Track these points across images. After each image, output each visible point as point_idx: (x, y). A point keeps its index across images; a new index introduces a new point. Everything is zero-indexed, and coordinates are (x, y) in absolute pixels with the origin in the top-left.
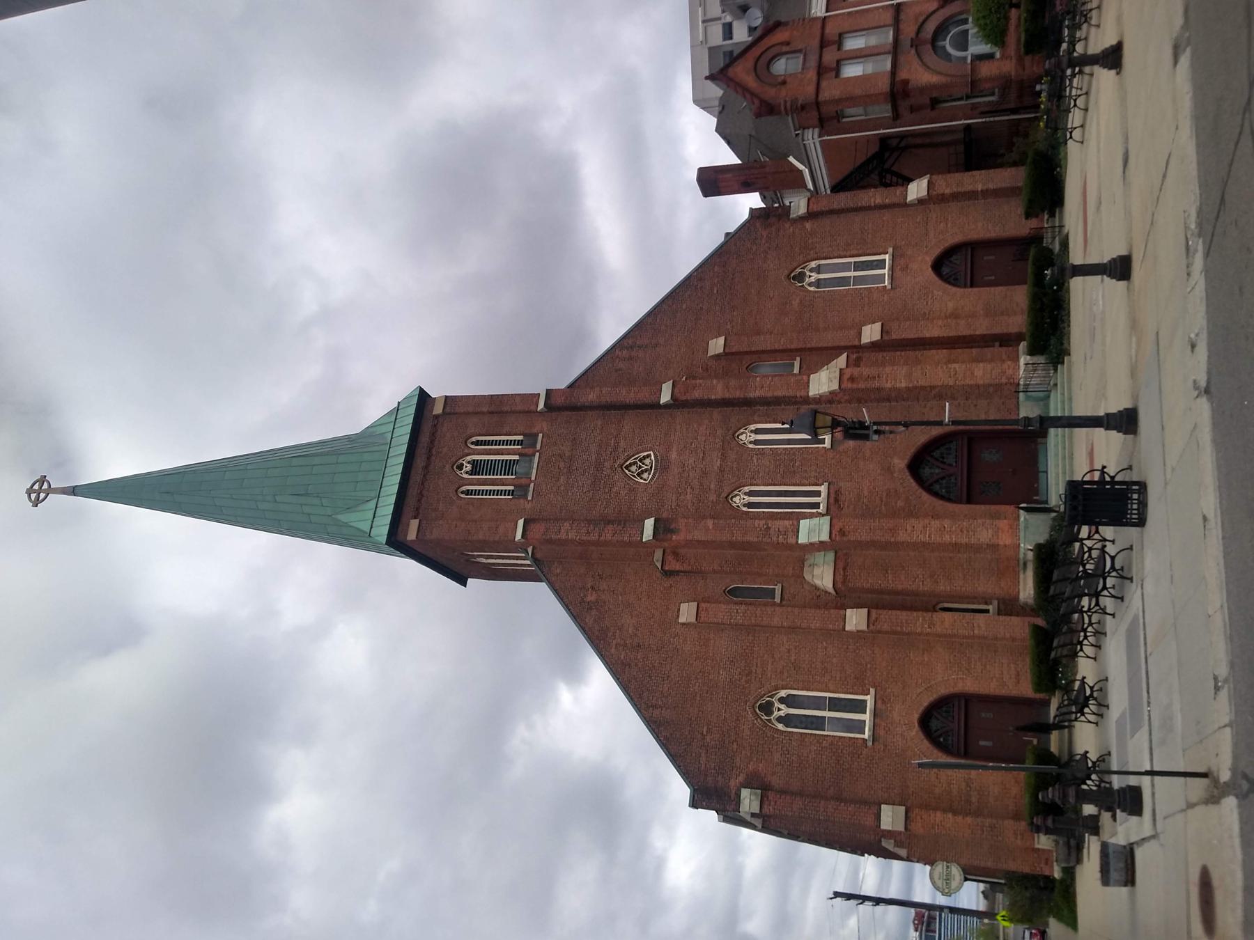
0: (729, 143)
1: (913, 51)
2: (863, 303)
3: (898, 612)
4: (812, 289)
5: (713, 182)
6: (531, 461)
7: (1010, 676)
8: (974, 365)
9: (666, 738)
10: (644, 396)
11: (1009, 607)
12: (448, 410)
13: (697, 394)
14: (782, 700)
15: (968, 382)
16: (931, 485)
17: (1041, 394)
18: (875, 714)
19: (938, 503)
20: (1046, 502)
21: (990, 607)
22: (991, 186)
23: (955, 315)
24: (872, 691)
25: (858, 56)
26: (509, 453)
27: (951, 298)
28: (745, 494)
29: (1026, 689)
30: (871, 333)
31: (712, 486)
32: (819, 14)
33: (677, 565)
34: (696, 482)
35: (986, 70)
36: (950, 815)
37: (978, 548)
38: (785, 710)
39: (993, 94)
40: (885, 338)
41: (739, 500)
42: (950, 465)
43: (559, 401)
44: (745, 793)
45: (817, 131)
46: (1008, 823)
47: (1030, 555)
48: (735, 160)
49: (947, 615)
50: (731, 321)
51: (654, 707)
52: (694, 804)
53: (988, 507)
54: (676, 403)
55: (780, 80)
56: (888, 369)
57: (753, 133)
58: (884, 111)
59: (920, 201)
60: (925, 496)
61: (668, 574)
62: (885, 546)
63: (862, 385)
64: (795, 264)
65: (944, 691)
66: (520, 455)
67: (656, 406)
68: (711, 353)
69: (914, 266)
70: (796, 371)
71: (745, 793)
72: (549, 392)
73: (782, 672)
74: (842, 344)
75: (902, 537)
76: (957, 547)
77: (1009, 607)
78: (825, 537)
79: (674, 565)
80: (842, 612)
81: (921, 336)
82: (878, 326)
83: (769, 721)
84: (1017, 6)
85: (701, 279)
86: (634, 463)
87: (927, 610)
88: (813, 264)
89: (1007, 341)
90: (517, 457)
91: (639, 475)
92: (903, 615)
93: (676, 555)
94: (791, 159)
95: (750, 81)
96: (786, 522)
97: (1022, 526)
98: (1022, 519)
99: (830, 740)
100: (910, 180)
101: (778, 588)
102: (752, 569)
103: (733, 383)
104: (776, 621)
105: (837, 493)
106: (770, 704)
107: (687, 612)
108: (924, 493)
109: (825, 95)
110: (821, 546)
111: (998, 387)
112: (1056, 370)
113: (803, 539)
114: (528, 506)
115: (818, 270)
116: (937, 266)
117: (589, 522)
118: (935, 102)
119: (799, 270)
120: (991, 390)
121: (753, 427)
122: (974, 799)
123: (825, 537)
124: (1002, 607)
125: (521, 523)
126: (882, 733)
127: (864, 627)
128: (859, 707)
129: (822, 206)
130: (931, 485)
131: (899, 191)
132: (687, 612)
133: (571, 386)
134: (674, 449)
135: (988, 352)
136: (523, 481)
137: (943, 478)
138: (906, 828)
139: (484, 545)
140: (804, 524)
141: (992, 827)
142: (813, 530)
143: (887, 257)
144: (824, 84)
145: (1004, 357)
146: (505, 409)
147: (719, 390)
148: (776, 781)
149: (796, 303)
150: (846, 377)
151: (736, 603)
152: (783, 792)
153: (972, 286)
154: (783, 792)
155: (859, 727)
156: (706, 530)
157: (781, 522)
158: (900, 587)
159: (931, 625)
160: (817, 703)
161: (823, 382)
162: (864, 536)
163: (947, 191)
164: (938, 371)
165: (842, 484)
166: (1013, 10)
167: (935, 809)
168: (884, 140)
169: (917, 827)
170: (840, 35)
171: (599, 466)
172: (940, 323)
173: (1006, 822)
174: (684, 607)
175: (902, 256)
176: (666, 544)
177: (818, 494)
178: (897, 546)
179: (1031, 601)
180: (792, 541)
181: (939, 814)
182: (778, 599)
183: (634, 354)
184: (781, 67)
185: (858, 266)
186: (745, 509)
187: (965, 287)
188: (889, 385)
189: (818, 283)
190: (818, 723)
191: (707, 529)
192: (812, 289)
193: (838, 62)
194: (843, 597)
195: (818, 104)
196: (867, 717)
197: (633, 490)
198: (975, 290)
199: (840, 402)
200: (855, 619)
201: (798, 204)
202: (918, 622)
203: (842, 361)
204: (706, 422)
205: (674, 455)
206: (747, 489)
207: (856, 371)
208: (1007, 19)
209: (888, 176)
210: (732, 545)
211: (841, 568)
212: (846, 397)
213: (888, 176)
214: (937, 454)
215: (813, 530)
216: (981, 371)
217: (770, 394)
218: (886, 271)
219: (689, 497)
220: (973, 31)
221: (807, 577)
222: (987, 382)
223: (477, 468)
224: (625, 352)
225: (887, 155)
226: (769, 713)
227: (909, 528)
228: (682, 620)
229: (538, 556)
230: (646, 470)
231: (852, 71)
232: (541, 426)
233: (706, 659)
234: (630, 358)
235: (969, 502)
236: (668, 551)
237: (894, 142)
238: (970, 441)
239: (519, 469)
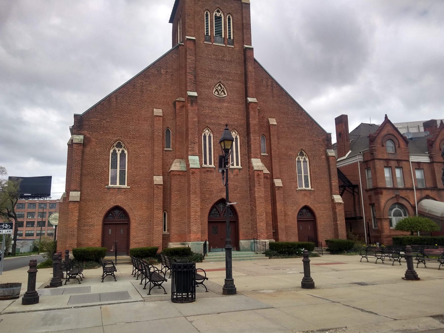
0: (357, 128)
1: (394, 196)
2: (292, 179)
3: (162, 196)
4: (297, 159)
5: (341, 121)
6: (221, 43)
7: (138, 239)
8: (265, 222)
9: (103, 104)
10: (251, 91)
11: (166, 239)
12: (244, 5)
13: (252, 113)
14: (123, 151)
15: (258, 220)
16: (216, 208)
18: (119, 188)
19: (208, 211)
20: (210, 251)
21: (166, 232)
22: (339, 227)
23: (286, 215)
24: (129, 187)
25: (393, 175)
26: (225, 33)
27: (292, 213)
28: (210, 135)
29: (133, 246)
30: (278, 183)
31: (212, 121)
32: (410, 159)
33: (179, 107)
34: (214, 114)
35: (386, 224)
36: (77, 219)
37: (189, 226)
38: (119, 153)
39: (375, 227)
40: (276, 188)
41: (207, 132)
43: (248, 54)
44: (82, 137)
45: (362, 160)
46: (75, 242)
47: (187, 246)
48: (350, 131)
49: (161, 215)
50: (283, 127)
51: (116, 99)
52: (76, 116)
53: (207, 229)
54: (248, 104)
55: (384, 144)
56: (263, 189)
57: (361, 137)
58: (370, 185)
59: (333, 200)
60: (211, 205)
61: (174, 104)
62: (189, 191)
63: (256, 179)
64: (307, 152)
65: (131, 215)
66: (224, 38)
67: (246, 96)
68: (270, 119)
69: (306, 198)
70: (262, 154)
71: (82, 137)
72: (252, 49)
73: (135, 151)
74: (274, 172)
75: (192, 196)
76: (189, 218)
77: (166, 239)
78: (191, 166)
79: (178, 106)
80: (161, 174)
81: (277, 202)
82: (281, 185)
83: (114, 146)
84: (412, 234)
85: (301, 114)
86: (222, 88)
87: (164, 207)
88: (307, 159)
89: (275, 235)
90: (223, 36)
91: (217, 90)
92: (161, 198)
93: (183, 107)
94: (350, 152)
95: (384, 133)
96: (197, 151)
97: (198, 242)
98: (201, 242)
99: (107, 171)
100: (341, 195)
101: (171, 149)
102: (178, 138)
103: (257, 128)
104: (156, 148)
105: (211, 171)
106: (121, 147)
107: (158, 112)
108: (212, 205)
109: (377, 162)
110: (188, 165)
111: (256, 231)
112: (263, 253)
113: (190, 157)
114: (201, 42)
115: (305, 161)
116: (306, 207)
117: (195, 68)
118: (372, 205)
119: (305, 154)
121: (238, 137)
122: (86, 228)
123: (191, 166)
124: (166, 236)
125: (194, 38)
126: (111, 191)
127: (155, 183)
128: (122, 182)
129: (332, 162)
130: (216, 208)
131: (337, 191)
132: (158, 112)
133: (255, 60)
134: (228, 105)
135: (271, 228)
136: (212, 39)
138: (70, 201)
139: (184, 24)
140: (197, 158)
141: (73, 235)
142: (194, 161)
143: (310, 188)
144: (382, 162)
145: (269, 234)
146: (245, 31)
147: (253, 122)
148: (88, 149)
149: (291, 153)
150: (259, 173)
151: (163, 132)
152: (83, 152)
153: (298, 221)
154: (83, 152)
155: (114, 182)
156: (193, 117)
157: (197, 149)
158: (172, 197)
159: (157, 209)
160: (122, 165)
161: (257, 164)
162: (192, 181)
163: (337, 210)
164: (262, 209)
165: (215, 173)
166: (409, 233)
167: (80, 213)
168: (357, 186)
169: (71, 206)
170: (402, 167)
171: (220, 72)
172: (283, 209)
173: (76, 240)
174: (161, 111)
175: (310, 194)
176: (187, 102)
177: (210, 163)
178: (189, 195)
179: (169, 247)
180: (190, 153)
181: (78, 214)
182: (165, 149)
183: (269, 87)
184: (389, 144)
185: (306, 177)
186: (203, 134)
187: (297, 218)
188: (256, 189)
189: (299, 162)
190: (114, 166)
191: (193, 118)
192: (297, 159)
193: (391, 167)
194: (168, 175)
195: (374, 159)
196: (118, 185)
197: (210, 87)
198: (296, 222)
199: (249, 171)
200: (158, 180)
201: (332, 153)
202: (158, 203)
203: (266, 171)
204: (240, 117)
205: (225, 104)
206: (212, 135)
207: (262, 177)
208: (407, 231)
209: (342, 189)
210: (187, 129)
211: (180, 173)
212: (251, 174)
213: (342, 189)
215: (194, 161)
216: (262, 225)
217: (252, 143)
218: (304, 188)
219: (208, 111)
220: (403, 218)
221: (176, 160)
223: (218, 19)
224: (270, 83)
225: (352, 188)
226: (117, 146)
227: (196, 199)
228: (155, 110)
229: (180, 47)
230: (219, 93)
231: (387, 173)
232: (237, 47)
233: (139, 120)
234: (267, 86)
235: (209, 222)
236: (184, 103)
237: (356, 190)
239: (218, 38)
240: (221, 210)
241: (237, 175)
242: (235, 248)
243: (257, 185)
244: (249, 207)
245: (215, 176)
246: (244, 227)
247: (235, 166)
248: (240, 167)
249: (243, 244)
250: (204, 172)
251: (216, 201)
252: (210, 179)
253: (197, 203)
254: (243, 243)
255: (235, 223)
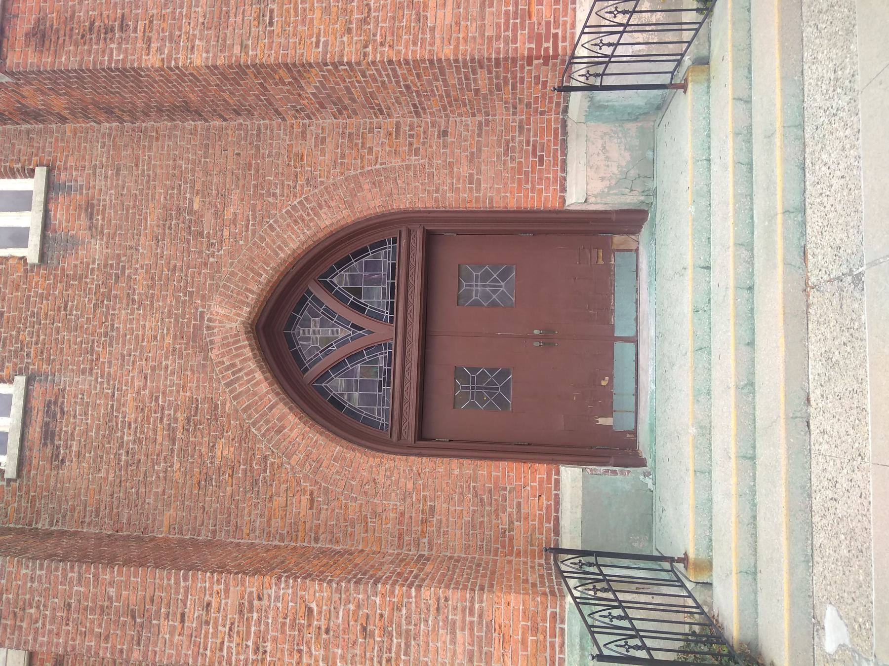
15: (407, 50)
16: (324, 376)
17: (637, 98)
42: (376, 316)
63: (69, 59)
111: (504, 69)
120: (482, 79)
130: (324, 376)
137: (354, 357)
165: (65, 379)
188: (152, 60)
214: (341, 280)
222: (467, 50)
227: (194, 613)
238: (430, 237)
240: (342, 332)
241: (90, 209)
242: (617, 239)
243: (115, 54)
244: (326, 121)
245: (84, 382)
246: (464, 170)
247: (30, 220)
248: (34, 185)
249: (597, 186)
250: (57, 461)
251: (264, 387)
252: (109, 417)
253: (232, 602)
254: (584, 187)
255: (433, 238)
